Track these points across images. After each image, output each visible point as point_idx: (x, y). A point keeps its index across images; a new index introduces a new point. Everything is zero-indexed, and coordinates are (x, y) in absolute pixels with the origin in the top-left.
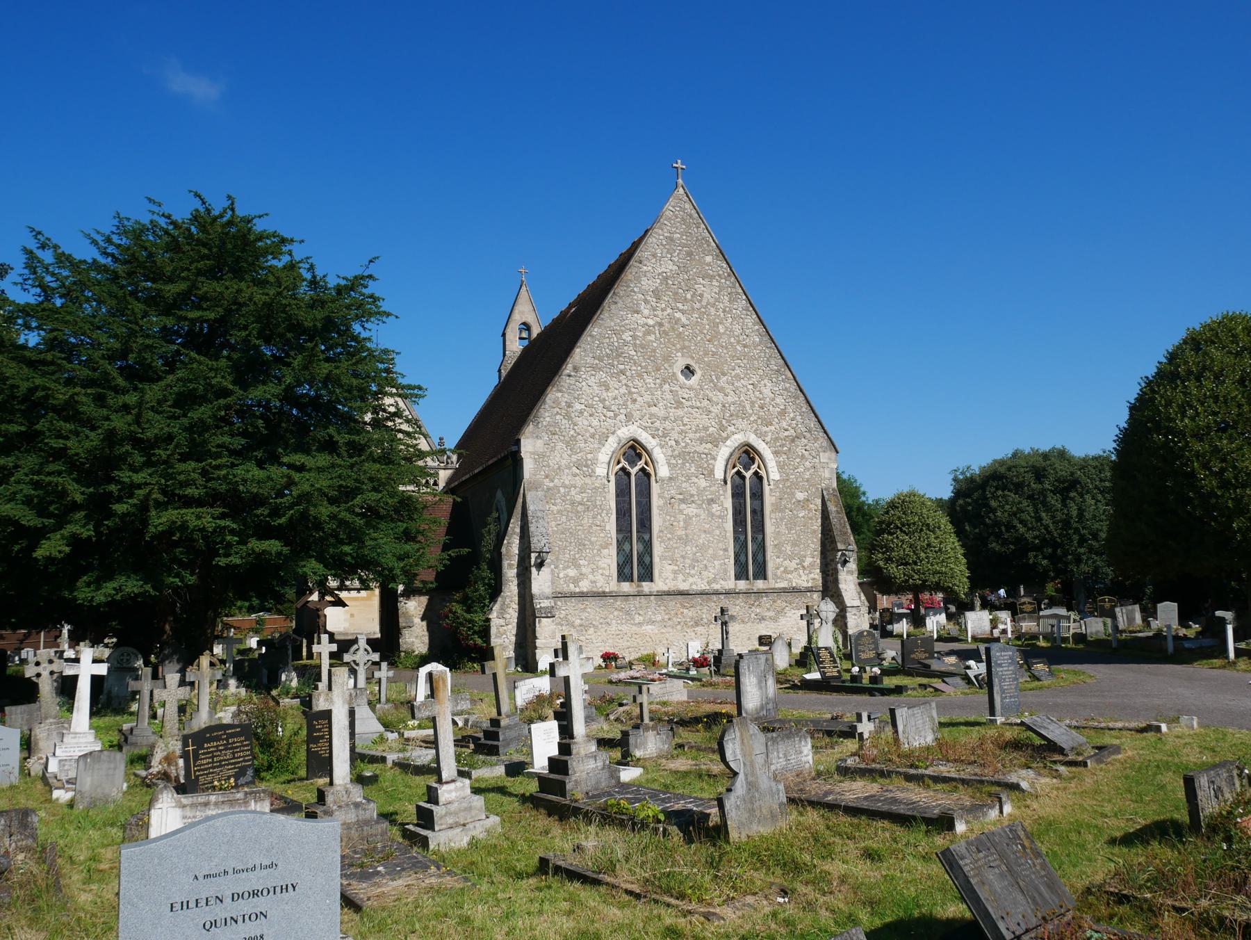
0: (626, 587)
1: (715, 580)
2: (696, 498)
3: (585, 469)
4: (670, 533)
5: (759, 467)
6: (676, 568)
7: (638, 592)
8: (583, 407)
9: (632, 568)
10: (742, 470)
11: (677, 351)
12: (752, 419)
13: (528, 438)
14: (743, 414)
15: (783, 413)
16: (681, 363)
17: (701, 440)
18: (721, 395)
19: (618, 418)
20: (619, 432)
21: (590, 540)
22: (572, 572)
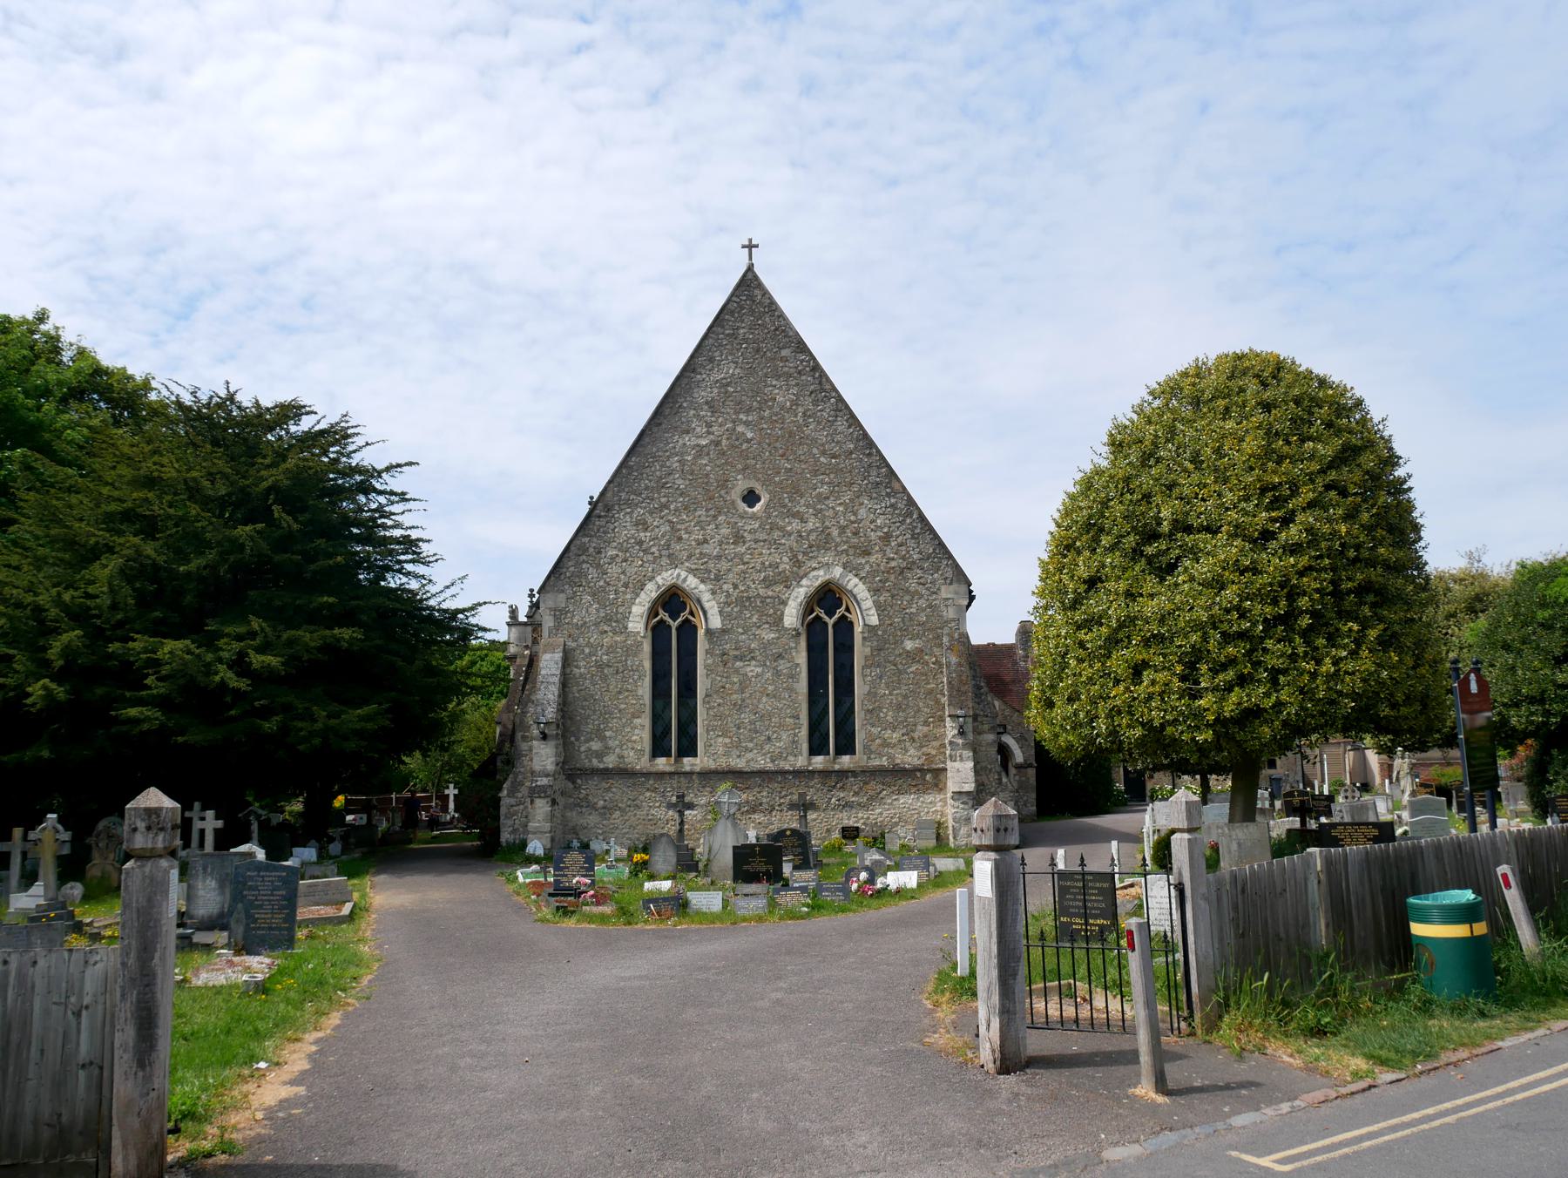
0: (662, 763)
1: (780, 756)
5: (848, 609)
10: (823, 615)
11: (739, 472)
12: (839, 549)
13: (548, 592)
14: (825, 542)
15: (887, 538)
16: (741, 485)
17: (768, 583)
18: (795, 525)
20: (659, 579)
22: (596, 746)
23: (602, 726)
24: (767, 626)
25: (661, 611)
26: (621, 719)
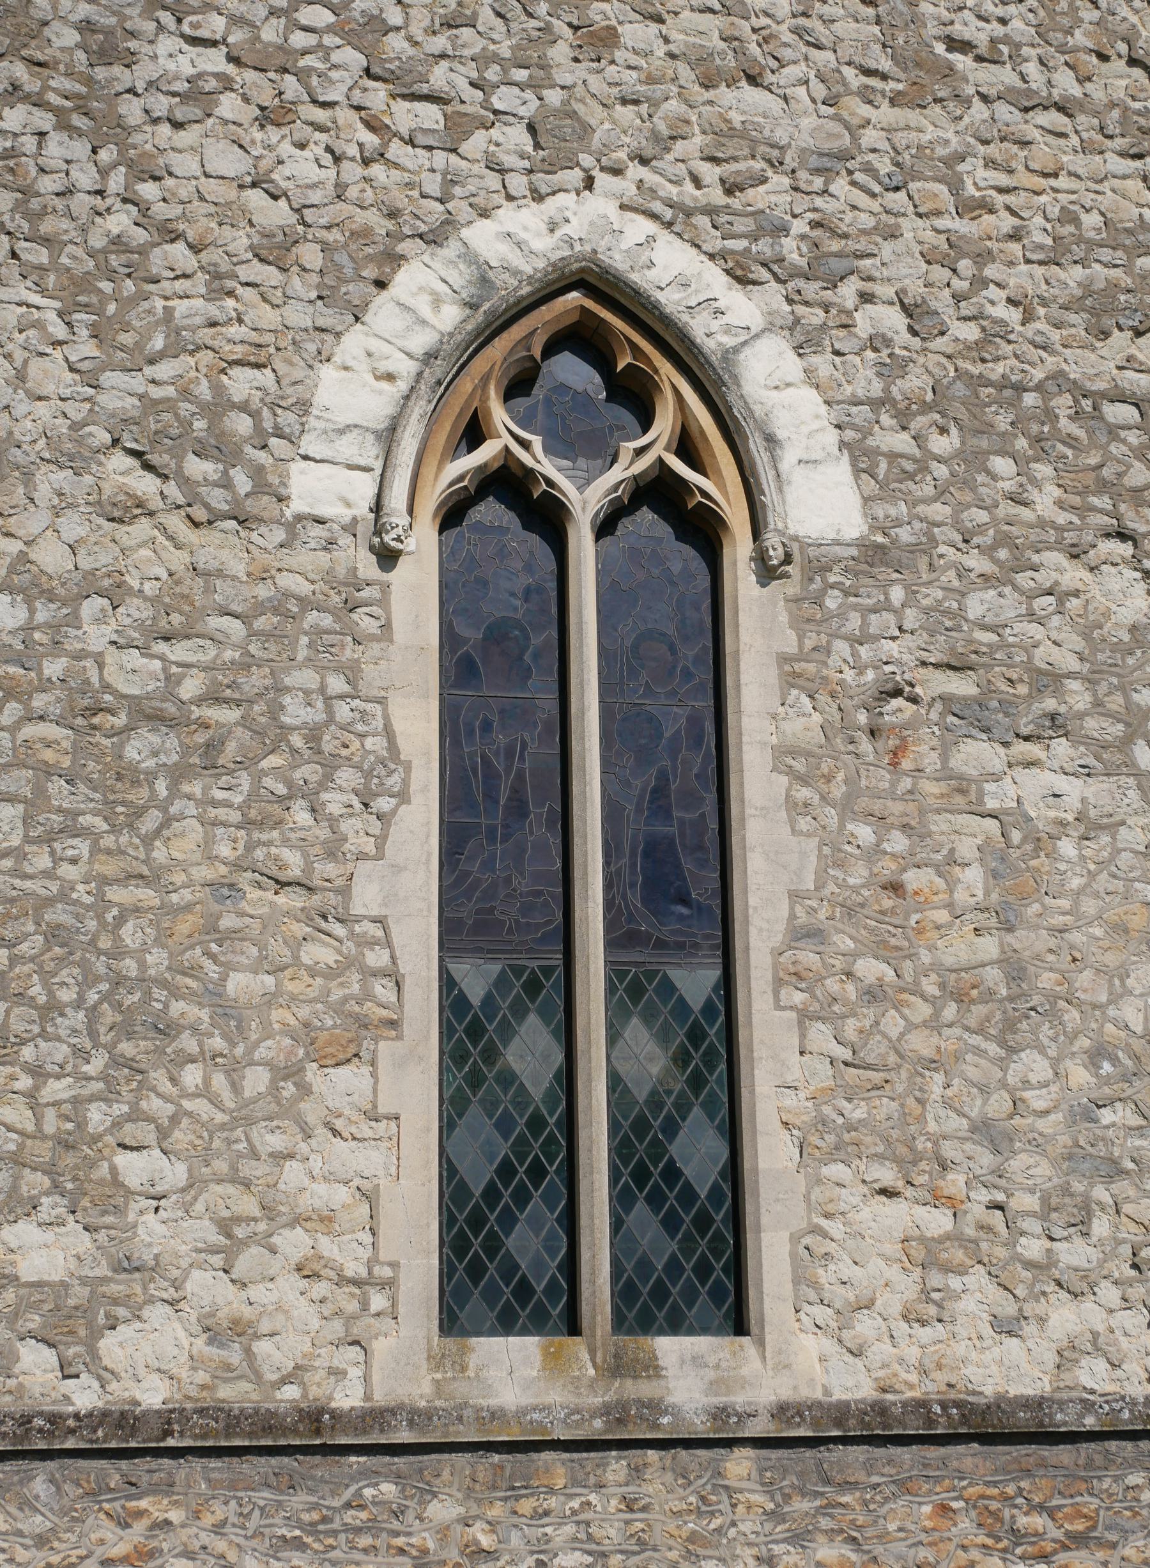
2: (1078, 697)
3: (197, 467)
4: (881, 949)
6: (939, 1221)
7: (618, 1413)
8: (214, 61)
9: (570, 1221)
19: (476, 143)
21: (214, 996)
23: (97, 1117)
24: (1127, 549)
25: (499, 415)
26: (234, 1072)
